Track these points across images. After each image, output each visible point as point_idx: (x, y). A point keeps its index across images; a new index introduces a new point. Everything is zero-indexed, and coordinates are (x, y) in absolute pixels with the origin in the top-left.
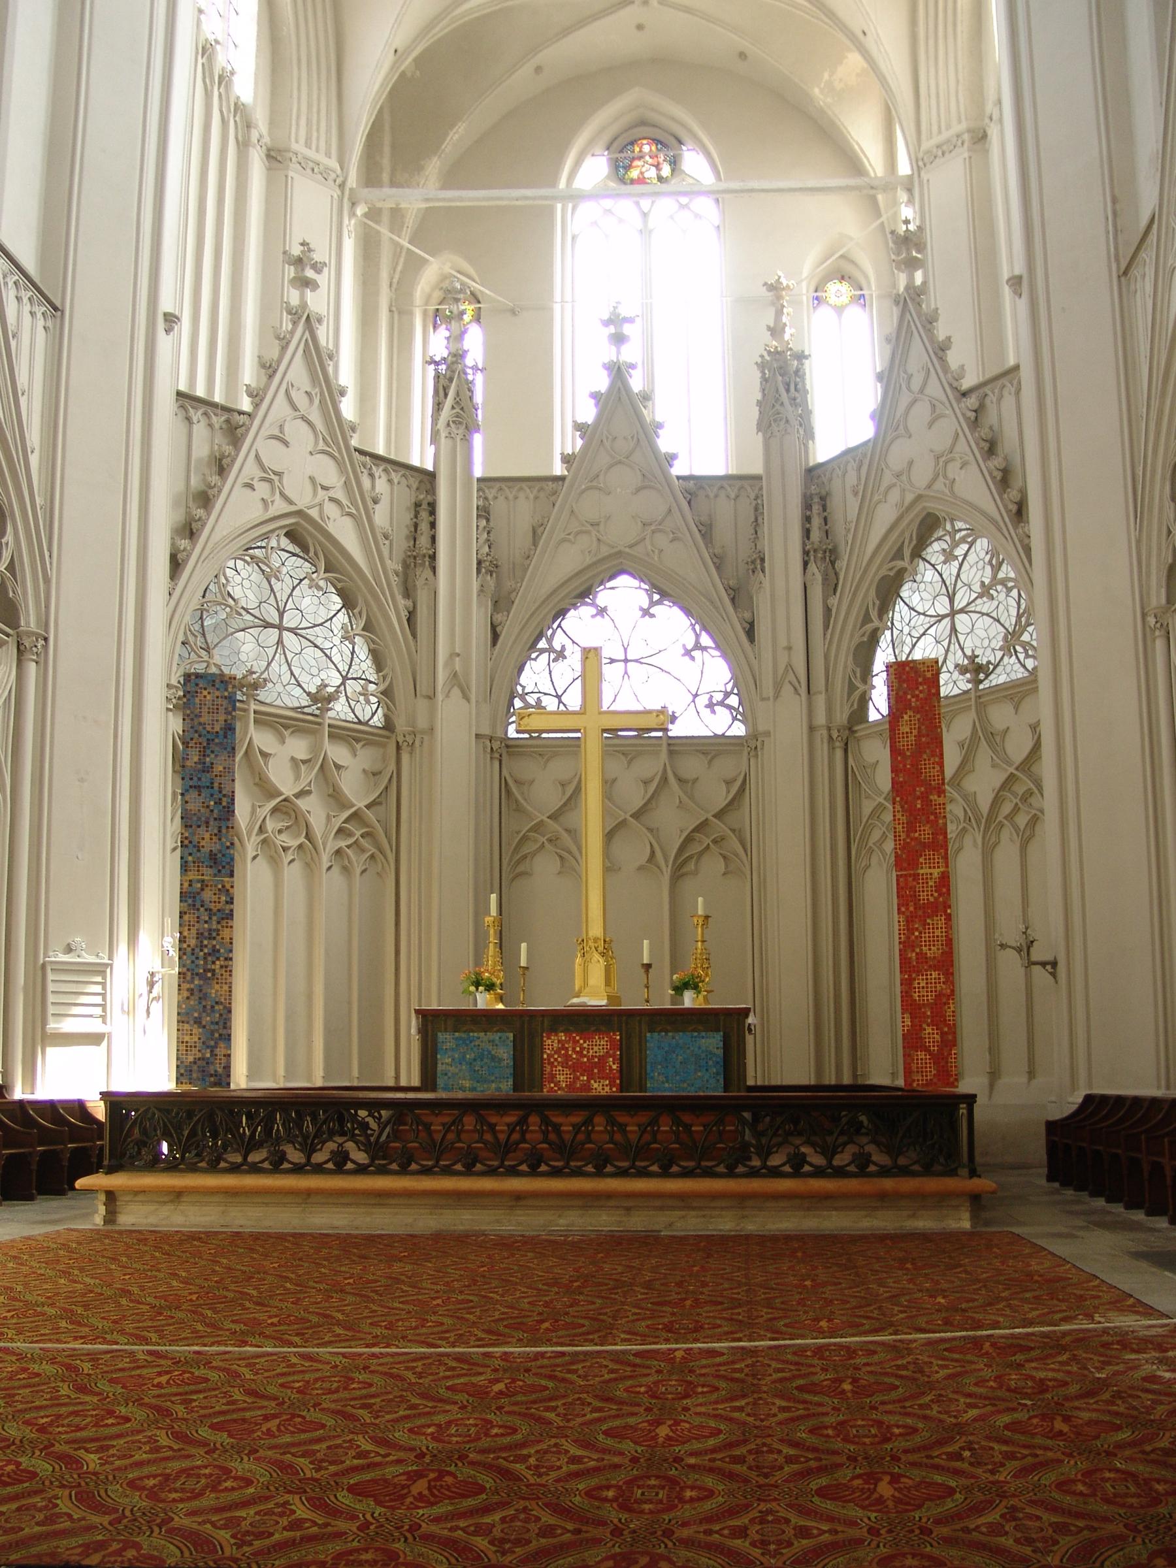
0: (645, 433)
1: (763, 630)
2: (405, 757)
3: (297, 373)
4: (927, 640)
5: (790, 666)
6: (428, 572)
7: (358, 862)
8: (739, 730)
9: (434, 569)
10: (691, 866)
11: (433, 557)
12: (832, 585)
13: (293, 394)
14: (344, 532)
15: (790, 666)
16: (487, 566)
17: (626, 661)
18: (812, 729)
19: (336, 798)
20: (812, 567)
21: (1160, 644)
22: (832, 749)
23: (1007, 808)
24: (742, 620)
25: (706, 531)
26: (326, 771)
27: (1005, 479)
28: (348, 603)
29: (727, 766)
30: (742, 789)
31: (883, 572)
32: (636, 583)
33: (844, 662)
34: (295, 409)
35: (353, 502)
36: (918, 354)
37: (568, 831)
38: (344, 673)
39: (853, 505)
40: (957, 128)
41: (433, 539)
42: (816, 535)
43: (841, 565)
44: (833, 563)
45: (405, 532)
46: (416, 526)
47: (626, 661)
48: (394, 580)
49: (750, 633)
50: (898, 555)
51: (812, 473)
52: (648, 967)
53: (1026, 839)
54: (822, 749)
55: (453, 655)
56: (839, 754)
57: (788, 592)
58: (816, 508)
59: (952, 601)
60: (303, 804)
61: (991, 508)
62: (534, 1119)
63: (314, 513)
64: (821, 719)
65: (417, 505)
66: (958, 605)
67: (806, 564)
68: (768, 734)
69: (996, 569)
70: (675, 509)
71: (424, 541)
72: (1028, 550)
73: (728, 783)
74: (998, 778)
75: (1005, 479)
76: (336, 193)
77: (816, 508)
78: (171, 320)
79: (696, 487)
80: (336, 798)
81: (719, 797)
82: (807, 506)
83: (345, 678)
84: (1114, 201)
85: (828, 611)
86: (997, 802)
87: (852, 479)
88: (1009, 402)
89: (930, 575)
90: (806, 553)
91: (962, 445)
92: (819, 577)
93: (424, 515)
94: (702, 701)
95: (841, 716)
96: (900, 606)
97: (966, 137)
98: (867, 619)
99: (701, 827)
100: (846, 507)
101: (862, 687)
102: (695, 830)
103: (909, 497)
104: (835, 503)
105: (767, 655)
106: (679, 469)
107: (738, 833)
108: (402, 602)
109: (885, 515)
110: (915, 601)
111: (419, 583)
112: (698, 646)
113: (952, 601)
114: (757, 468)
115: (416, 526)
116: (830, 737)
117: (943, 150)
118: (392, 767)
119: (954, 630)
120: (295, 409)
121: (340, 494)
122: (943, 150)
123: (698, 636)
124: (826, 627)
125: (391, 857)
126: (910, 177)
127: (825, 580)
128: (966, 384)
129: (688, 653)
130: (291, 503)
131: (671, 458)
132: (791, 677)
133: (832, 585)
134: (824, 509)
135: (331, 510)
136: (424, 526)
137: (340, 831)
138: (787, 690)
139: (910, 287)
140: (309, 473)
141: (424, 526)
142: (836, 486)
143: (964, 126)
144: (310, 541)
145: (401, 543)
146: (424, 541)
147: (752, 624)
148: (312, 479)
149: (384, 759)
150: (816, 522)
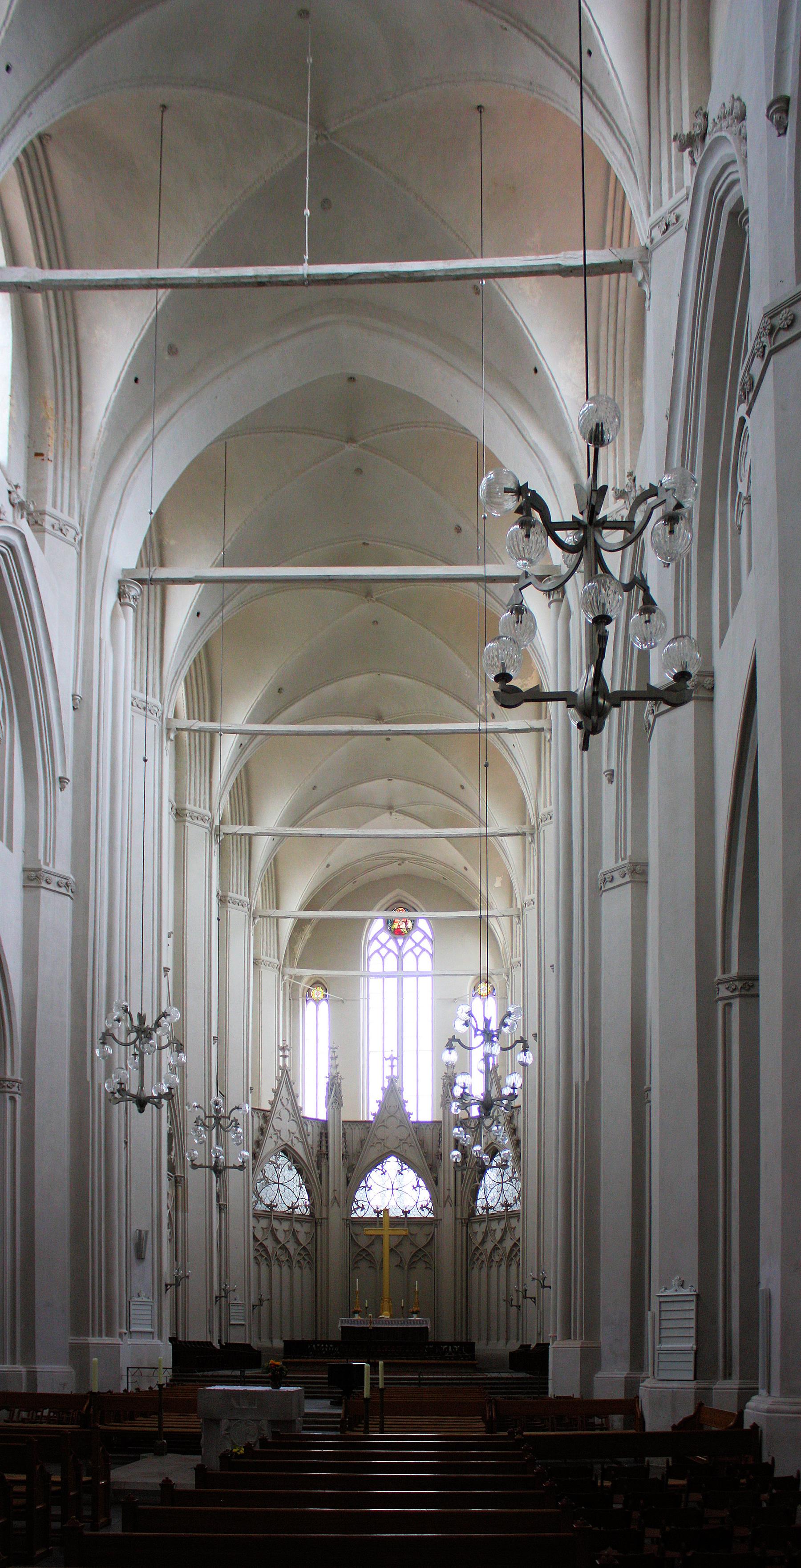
0: (401, 1104)
3: (284, 1093)
5: (449, 1196)
6: (325, 1160)
8: (431, 1216)
9: (328, 1159)
11: (327, 1155)
13: (283, 1100)
14: (299, 1149)
15: (449, 1196)
16: (345, 1156)
17: (393, 1189)
18: (456, 1219)
19: (298, 1242)
22: (462, 1226)
25: (422, 1143)
26: (294, 1233)
28: (299, 1171)
29: (427, 1229)
33: (468, 1195)
34: (283, 1105)
35: (302, 1137)
38: (297, 1195)
41: (327, 1147)
45: (317, 1144)
46: (321, 1142)
47: (393, 1189)
48: (315, 1164)
49: (436, 1182)
54: (459, 1226)
56: (465, 1228)
60: (287, 1245)
63: (290, 1143)
64: (459, 1216)
65: (321, 1133)
68: (441, 1220)
70: (411, 1135)
71: (324, 1148)
79: (419, 1126)
80: (298, 1242)
83: (298, 1199)
85: (462, 1176)
93: (324, 1138)
94: (419, 1206)
95: (466, 1216)
106: (413, 1118)
108: (318, 1172)
111: (323, 1164)
114: (441, 1119)
115: (321, 1142)
116: (462, 1223)
118: (314, 1230)
120: (283, 1105)
121: (297, 1135)
124: (462, 1182)
129: (414, 1188)
130: (283, 1141)
131: (410, 1114)
135: (295, 1141)
136: (324, 1142)
137: (299, 1254)
138: (448, 1204)
140: (288, 1128)
141: (324, 1142)
144: (304, 1172)
145: (316, 1149)
146: (324, 1148)
148: (289, 1131)
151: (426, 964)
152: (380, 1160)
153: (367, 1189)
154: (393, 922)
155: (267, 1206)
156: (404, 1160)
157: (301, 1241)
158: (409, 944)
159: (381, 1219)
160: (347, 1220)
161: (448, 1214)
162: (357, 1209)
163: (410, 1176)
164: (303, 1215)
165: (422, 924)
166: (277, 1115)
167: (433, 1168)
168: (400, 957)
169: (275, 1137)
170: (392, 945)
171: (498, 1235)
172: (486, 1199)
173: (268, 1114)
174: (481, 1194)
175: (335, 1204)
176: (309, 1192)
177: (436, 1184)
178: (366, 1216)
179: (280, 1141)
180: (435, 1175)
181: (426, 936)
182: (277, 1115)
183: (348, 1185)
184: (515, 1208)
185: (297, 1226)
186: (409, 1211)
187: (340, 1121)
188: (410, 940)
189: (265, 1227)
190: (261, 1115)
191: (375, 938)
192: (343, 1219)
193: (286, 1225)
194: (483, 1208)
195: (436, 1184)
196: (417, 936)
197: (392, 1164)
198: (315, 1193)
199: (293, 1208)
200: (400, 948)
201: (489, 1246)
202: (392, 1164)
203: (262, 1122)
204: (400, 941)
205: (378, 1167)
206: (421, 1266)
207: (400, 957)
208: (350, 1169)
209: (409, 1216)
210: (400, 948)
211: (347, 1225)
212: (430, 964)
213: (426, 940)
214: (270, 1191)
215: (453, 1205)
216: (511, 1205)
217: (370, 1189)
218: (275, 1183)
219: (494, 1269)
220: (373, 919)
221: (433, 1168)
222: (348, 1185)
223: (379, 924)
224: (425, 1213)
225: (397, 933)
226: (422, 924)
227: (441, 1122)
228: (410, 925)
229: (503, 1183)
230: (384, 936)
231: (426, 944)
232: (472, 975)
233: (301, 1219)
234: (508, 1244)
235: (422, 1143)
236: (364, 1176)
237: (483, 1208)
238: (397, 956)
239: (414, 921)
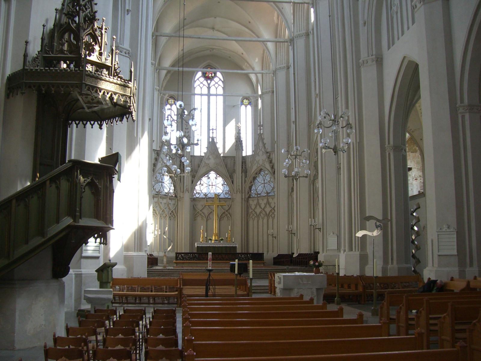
1: (235, 182)
2: (179, 202)
4: (260, 186)
7: (172, 218)
10: (222, 219)
12: (246, 177)
20: (243, 173)
21: (290, 197)
23: (271, 214)
24: (231, 180)
27: (272, 167)
30: (230, 207)
31: (254, 176)
32: (214, 173)
33: (247, 189)
36: (261, 144)
37: (203, 213)
39: (250, 166)
40: (269, 90)
42: (244, 168)
43: (248, 174)
44: (246, 173)
50: (256, 174)
51: (243, 157)
52: (227, 238)
53: (273, 218)
55: (186, 186)
57: (258, 239)
58: (244, 164)
59: (264, 181)
61: (270, 170)
62: (220, 255)
66: (265, 182)
67: (242, 173)
68: (235, 199)
69: (270, 179)
72: (275, 178)
73: (228, 206)
74: (270, 209)
75: (272, 167)
76: (158, 92)
77: (244, 164)
78: (154, 141)
81: (227, 208)
82: (242, 163)
83: (170, 189)
84: (288, 135)
85: (245, 180)
86: (269, 213)
87: (250, 160)
88: (274, 155)
89: (261, 177)
90: (242, 171)
91: (266, 160)
92: (244, 175)
96: (256, 180)
97: (271, 92)
98: (251, 183)
99: (224, 213)
100: (249, 164)
101: (250, 193)
102: (223, 213)
103: (259, 165)
104: (247, 162)
105: (235, 186)
107: (229, 213)
109: (255, 168)
110: (259, 180)
112: (224, 184)
113: (264, 181)
117: (266, 93)
118: (177, 203)
119: (264, 186)
122: (266, 93)
123: (224, 183)
125: (177, 218)
126: (261, 95)
127: (245, 176)
128: (268, 151)
132: (239, 190)
133: (246, 177)
134: (245, 164)
139: (260, 133)
142: (247, 160)
143: (270, 90)
147: (233, 181)
149: (175, 202)
150: (244, 166)
151: (220, 91)
152: (207, 173)
153: (201, 185)
154: (206, 73)
155: (157, 192)
156: (219, 173)
157: (171, 208)
158: (213, 83)
159: (206, 198)
160: (192, 199)
161: (238, 197)
162: (196, 194)
163: (220, 180)
164: (172, 196)
165: (219, 74)
166: (163, 153)
167: (231, 177)
168: (209, 88)
169: (161, 162)
170: (205, 83)
171: (263, 206)
172: (256, 190)
173: (159, 152)
174: (253, 188)
175: (187, 191)
176: (174, 186)
177: (233, 183)
178: (200, 197)
179: (164, 164)
180: (232, 180)
181: (220, 80)
182: (163, 153)
183: (192, 183)
184: (270, 194)
185: (170, 201)
186: (220, 195)
187: (189, 155)
188: (213, 81)
189: (156, 201)
190: (156, 152)
191: (198, 79)
192: (190, 198)
193: (165, 201)
194: (256, 194)
195: (233, 183)
196: (216, 79)
197: (212, 174)
198: (178, 187)
199: (168, 193)
200: (209, 84)
201: (258, 210)
202: (212, 174)
203: (156, 155)
204: (209, 81)
205: (206, 176)
206: (225, 218)
207: (209, 88)
208: (193, 177)
209: (220, 197)
210: (209, 84)
211: (192, 201)
212: (222, 91)
213: (220, 81)
214: (158, 186)
215: (241, 193)
216: (269, 193)
217: (202, 185)
218: (160, 182)
219: (261, 221)
220: (197, 72)
221: (231, 177)
222: (192, 183)
223: (200, 74)
224: (226, 196)
225: (207, 78)
226: (219, 74)
227: (235, 157)
228: (213, 75)
229: (264, 183)
230: (202, 79)
231: (221, 83)
232: (241, 96)
233: (171, 198)
234: (268, 209)
235: (226, 166)
236: (200, 179)
237: (256, 194)
238: (208, 88)
239: (215, 74)
